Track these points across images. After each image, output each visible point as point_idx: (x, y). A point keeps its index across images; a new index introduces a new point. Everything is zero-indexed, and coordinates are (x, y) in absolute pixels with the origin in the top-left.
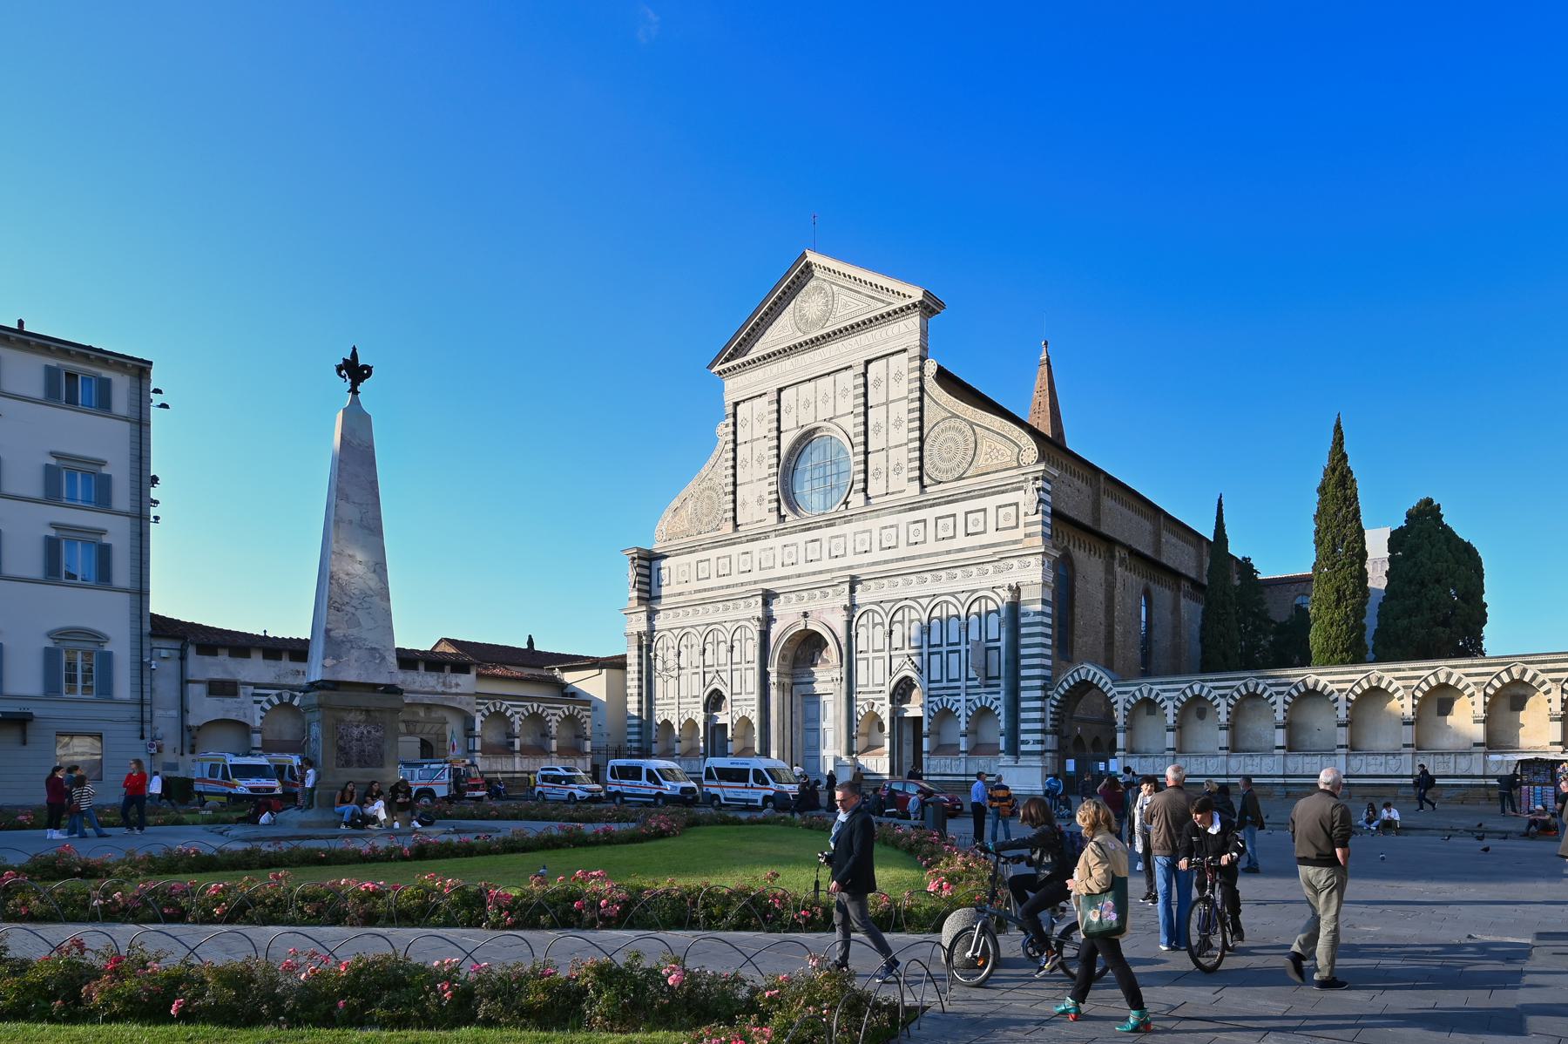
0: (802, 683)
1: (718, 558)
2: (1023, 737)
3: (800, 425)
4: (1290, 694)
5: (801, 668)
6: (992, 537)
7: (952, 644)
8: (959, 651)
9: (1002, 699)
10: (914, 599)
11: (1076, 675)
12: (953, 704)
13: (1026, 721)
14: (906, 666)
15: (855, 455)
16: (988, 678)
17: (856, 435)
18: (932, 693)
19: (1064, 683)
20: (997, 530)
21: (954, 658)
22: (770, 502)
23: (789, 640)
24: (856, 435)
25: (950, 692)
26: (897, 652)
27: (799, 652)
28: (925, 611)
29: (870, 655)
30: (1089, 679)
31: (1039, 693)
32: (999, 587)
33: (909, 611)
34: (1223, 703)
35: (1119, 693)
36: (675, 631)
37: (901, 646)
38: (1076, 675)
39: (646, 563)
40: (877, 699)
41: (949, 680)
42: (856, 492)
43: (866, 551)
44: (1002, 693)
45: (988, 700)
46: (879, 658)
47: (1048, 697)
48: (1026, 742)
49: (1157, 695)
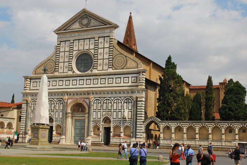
2: (137, 134)
3: (79, 49)
4: (199, 127)
7: (119, 110)
9: (132, 124)
10: (110, 97)
12: (119, 125)
13: (138, 130)
14: (107, 114)
16: (128, 119)
17: (95, 55)
18: (114, 121)
19: (148, 121)
21: (120, 113)
22: (69, 68)
23: (73, 105)
24: (95, 55)
25: (118, 121)
26: (104, 110)
30: (154, 120)
35: (161, 124)
39: (29, 80)
41: (118, 118)
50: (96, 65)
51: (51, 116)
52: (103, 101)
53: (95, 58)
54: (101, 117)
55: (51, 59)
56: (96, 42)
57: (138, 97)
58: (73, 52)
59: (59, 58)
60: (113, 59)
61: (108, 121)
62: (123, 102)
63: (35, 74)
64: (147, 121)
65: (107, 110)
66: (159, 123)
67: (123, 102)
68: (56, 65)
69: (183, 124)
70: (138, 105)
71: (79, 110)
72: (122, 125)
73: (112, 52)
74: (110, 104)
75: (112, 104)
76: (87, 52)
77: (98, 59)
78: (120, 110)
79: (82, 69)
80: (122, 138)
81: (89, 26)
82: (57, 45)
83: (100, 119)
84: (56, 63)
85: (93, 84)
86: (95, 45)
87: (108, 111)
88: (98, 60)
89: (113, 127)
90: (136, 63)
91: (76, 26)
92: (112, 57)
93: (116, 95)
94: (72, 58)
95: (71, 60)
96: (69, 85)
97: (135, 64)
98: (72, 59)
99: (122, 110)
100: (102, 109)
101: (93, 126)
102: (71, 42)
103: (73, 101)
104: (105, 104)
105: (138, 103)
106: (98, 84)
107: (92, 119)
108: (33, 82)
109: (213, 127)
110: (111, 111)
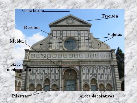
1: (48, 54)
10: (94, 65)
21: (102, 75)
42: (79, 48)
44: (112, 82)
48: (118, 89)
51: (48, 78)
59: (52, 40)
60: (91, 43)
71: (69, 74)
75: (97, 69)
76: (72, 38)
82: (50, 33)
92: (90, 42)
99: (104, 74)
100: (89, 73)
102: (61, 31)
105: (115, 69)
108: (31, 54)
110: (96, 75)
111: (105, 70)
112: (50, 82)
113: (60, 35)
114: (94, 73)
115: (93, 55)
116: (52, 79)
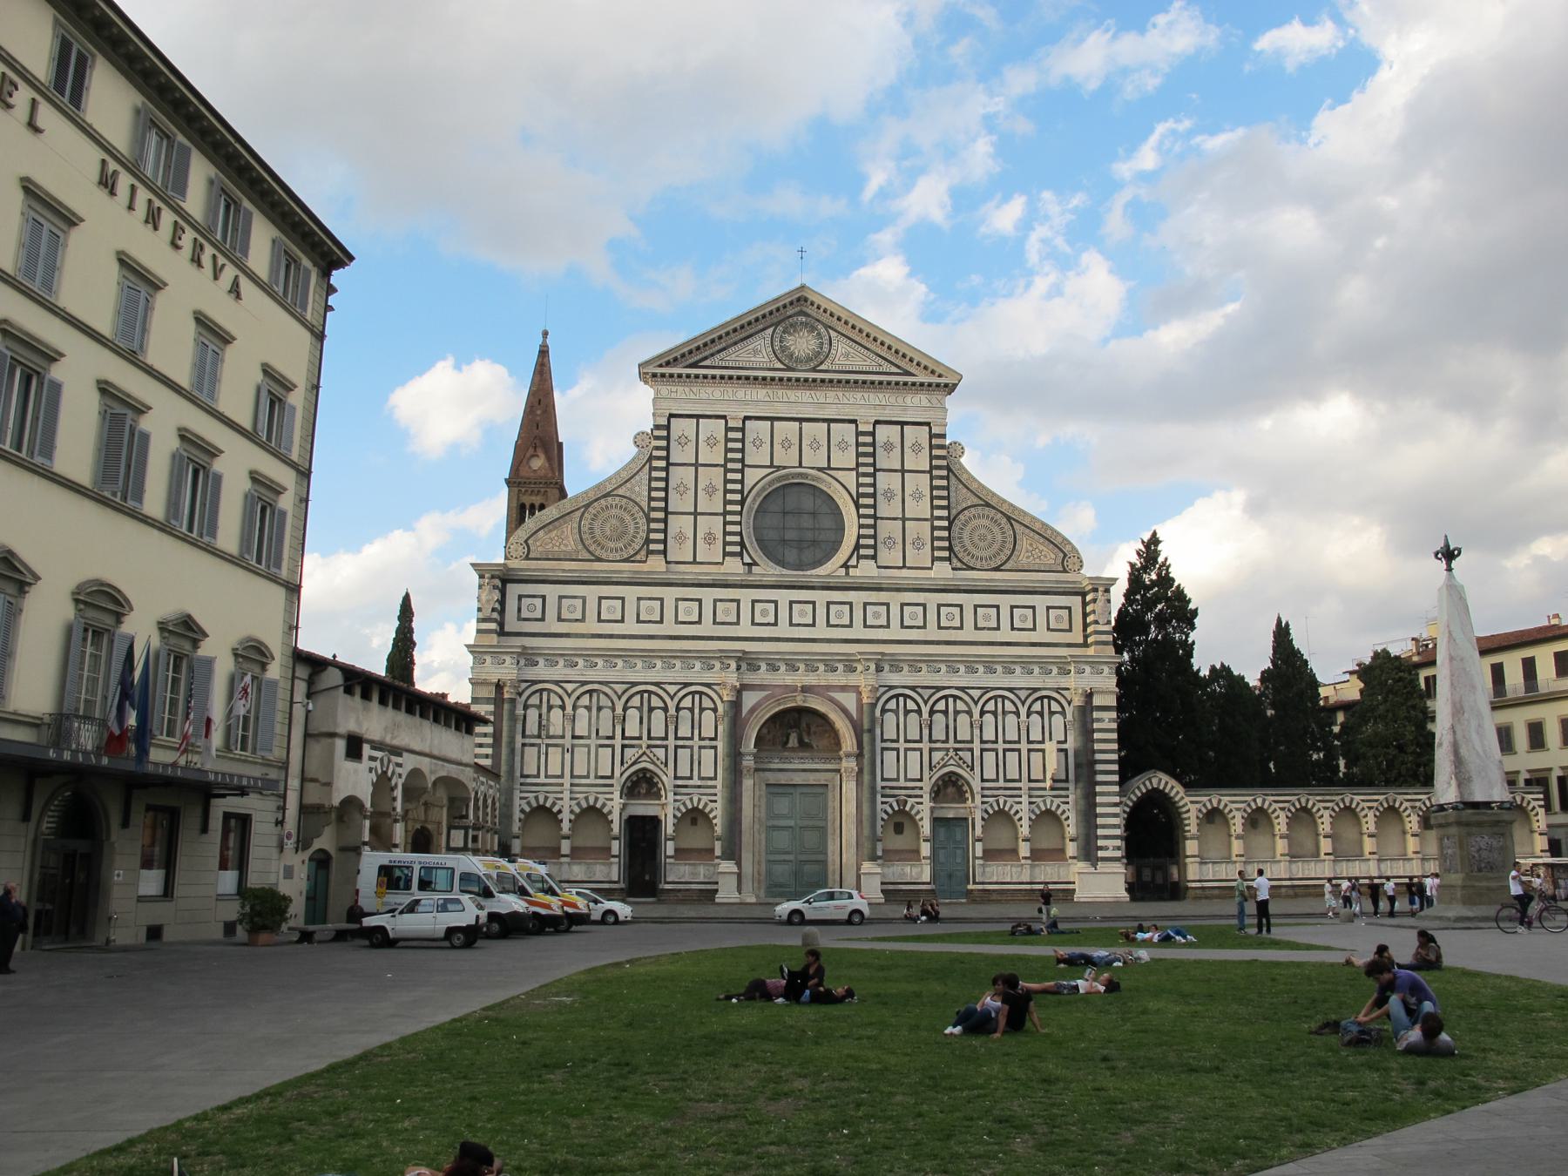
0: (770, 770)
2: (1100, 843)
4: (1333, 810)
5: (766, 750)
6: (1041, 635)
7: (1010, 742)
8: (1019, 750)
10: (962, 689)
11: (1147, 783)
12: (1012, 807)
13: (1104, 826)
14: (952, 762)
15: (860, 516)
16: (1054, 781)
17: (860, 495)
18: (987, 792)
20: (1048, 629)
21: (1012, 758)
27: (765, 731)
28: (976, 703)
29: (902, 745)
30: (1161, 788)
31: (1117, 799)
32: (1068, 689)
33: (955, 701)
34: (1282, 815)
35: (1192, 802)
36: (570, 687)
37: (944, 738)
38: (1147, 783)
40: (910, 796)
41: (1006, 780)
42: (859, 557)
43: (881, 627)
44: (1071, 799)
45: (1053, 804)
46: (914, 749)
47: (1121, 803)
48: (1106, 848)
49: (1226, 805)
50: (871, 542)
51: (651, 767)
52: (931, 702)
53: (862, 511)
54: (926, 776)
55: (620, 492)
56: (861, 439)
57: (1098, 692)
58: (742, 471)
59: (666, 490)
60: (951, 523)
61: (951, 790)
62: (1023, 711)
63: (527, 558)
64: (1133, 792)
65: (951, 744)
66: (1182, 798)
67: (1023, 711)
68: (653, 526)
69: (1275, 802)
70: (1096, 726)
71: (787, 742)
72: (1025, 806)
73: (945, 493)
74: (963, 720)
77: (875, 517)
78: (1015, 742)
79: (791, 555)
80: (1029, 862)
81: (822, 367)
83: (918, 784)
84: (654, 515)
85: (865, 626)
86: (858, 455)
87: (956, 750)
88: (879, 521)
89: (983, 819)
90: (1056, 550)
91: (757, 354)
92: (945, 513)
93: (991, 681)
94: (738, 497)
95: (738, 508)
96: (738, 623)
97: (1053, 556)
98: (742, 503)
99: (1024, 746)
101: (886, 812)
103: (766, 698)
104: (939, 718)
105: (1096, 715)
106: (888, 626)
107: (880, 783)
108: (520, 597)
109: (1381, 809)
110: (971, 750)
111: (1035, 718)
112: (659, 797)
113: (727, 450)
114: (956, 741)
115: (956, 611)
116: (676, 778)
